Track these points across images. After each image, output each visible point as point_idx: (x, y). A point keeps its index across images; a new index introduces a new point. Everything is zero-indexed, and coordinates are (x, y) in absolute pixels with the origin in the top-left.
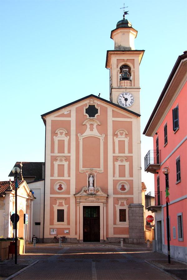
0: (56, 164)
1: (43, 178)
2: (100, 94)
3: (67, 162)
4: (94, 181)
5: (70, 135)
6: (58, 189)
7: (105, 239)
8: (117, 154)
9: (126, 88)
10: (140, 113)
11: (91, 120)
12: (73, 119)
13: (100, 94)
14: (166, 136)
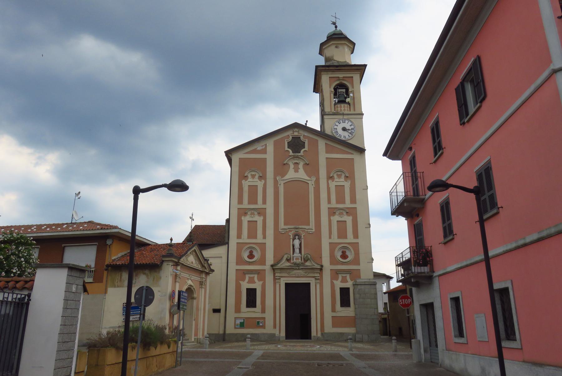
0: (245, 220)
1: (226, 241)
2: (307, 121)
3: (262, 218)
4: (300, 245)
5: (266, 178)
6: (249, 257)
7: (319, 335)
8: (334, 204)
9: (343, 114)
10: (365, 147)
11: (294, 157)
12: (270, 157)
13: (307, 121)
14: (437, 141)
